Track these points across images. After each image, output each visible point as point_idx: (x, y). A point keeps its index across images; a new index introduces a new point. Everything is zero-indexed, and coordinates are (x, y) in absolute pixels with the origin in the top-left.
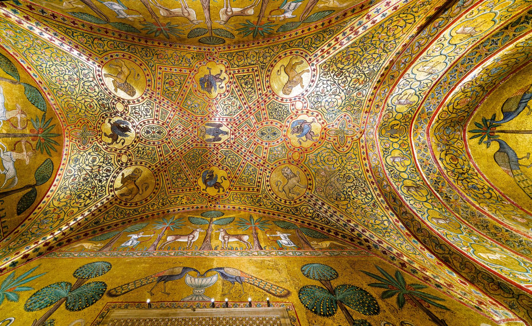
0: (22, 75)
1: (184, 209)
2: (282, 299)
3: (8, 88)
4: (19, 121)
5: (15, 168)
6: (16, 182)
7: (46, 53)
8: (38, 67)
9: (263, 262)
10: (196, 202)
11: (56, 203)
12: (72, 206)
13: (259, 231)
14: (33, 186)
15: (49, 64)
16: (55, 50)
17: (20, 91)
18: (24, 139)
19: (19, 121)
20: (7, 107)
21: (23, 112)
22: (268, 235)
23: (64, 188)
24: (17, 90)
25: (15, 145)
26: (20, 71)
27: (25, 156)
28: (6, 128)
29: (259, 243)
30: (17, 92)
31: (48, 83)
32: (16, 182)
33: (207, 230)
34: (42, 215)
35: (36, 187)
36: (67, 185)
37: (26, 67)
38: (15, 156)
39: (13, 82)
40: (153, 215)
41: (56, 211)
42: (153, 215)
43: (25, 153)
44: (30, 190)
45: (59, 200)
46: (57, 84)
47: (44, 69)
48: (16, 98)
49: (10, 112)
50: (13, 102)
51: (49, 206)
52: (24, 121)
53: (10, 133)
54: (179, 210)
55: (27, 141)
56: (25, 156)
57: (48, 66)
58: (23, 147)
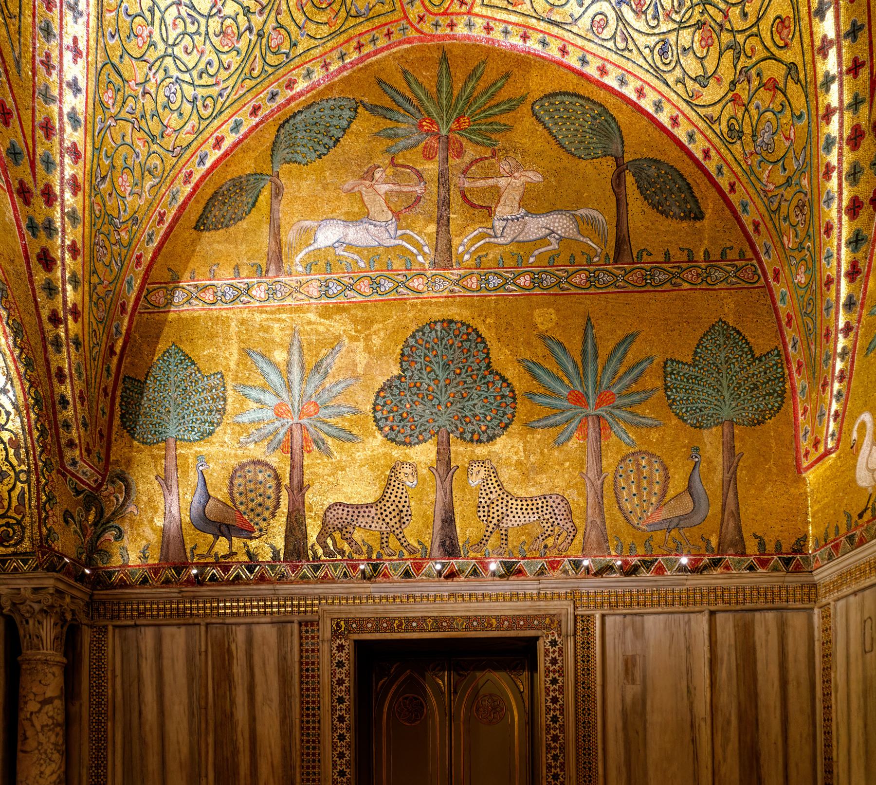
0: (247, 165)
3: (297, 207)
4: (396, 188)
5: (548, 213)
6: (595, 213)
7: (140, 79)
8: (205, 113)
11: (711, 93)
12: (752, 19)
14: (620, 168)
15: (174, 73)
16: (112, 42)
17: (300, 177)
18: (455, 180)
19: (396, 188)
20: (354, 214)
21: (369, 175)
23: (663, 53)
24: (299, 184)
25: (473, 206)
26: (234, 171)
27: (512, 183)
28: (420, 224)
30: (304, 185)
31: (249, 83)
32: (595, 213)
34: (737, 148)
35: (628, 158)
36: (652, 41)
37: (218, 153)
38: (508, 209)
39: (278, 192)
41: (745, 97)
43: (502, 182)
44: (629, 179)
45: (702, 80)
46: (242, 45)
47: (201, 92)
48: (325, 188)
49: (372, 210)
50: (338, 198)
51: (710, 120)
52: (395, 174)
53: (435, 215)
55: (464, 172)
56: (512, 183)
57: (187, 77)
58: (481, 183)
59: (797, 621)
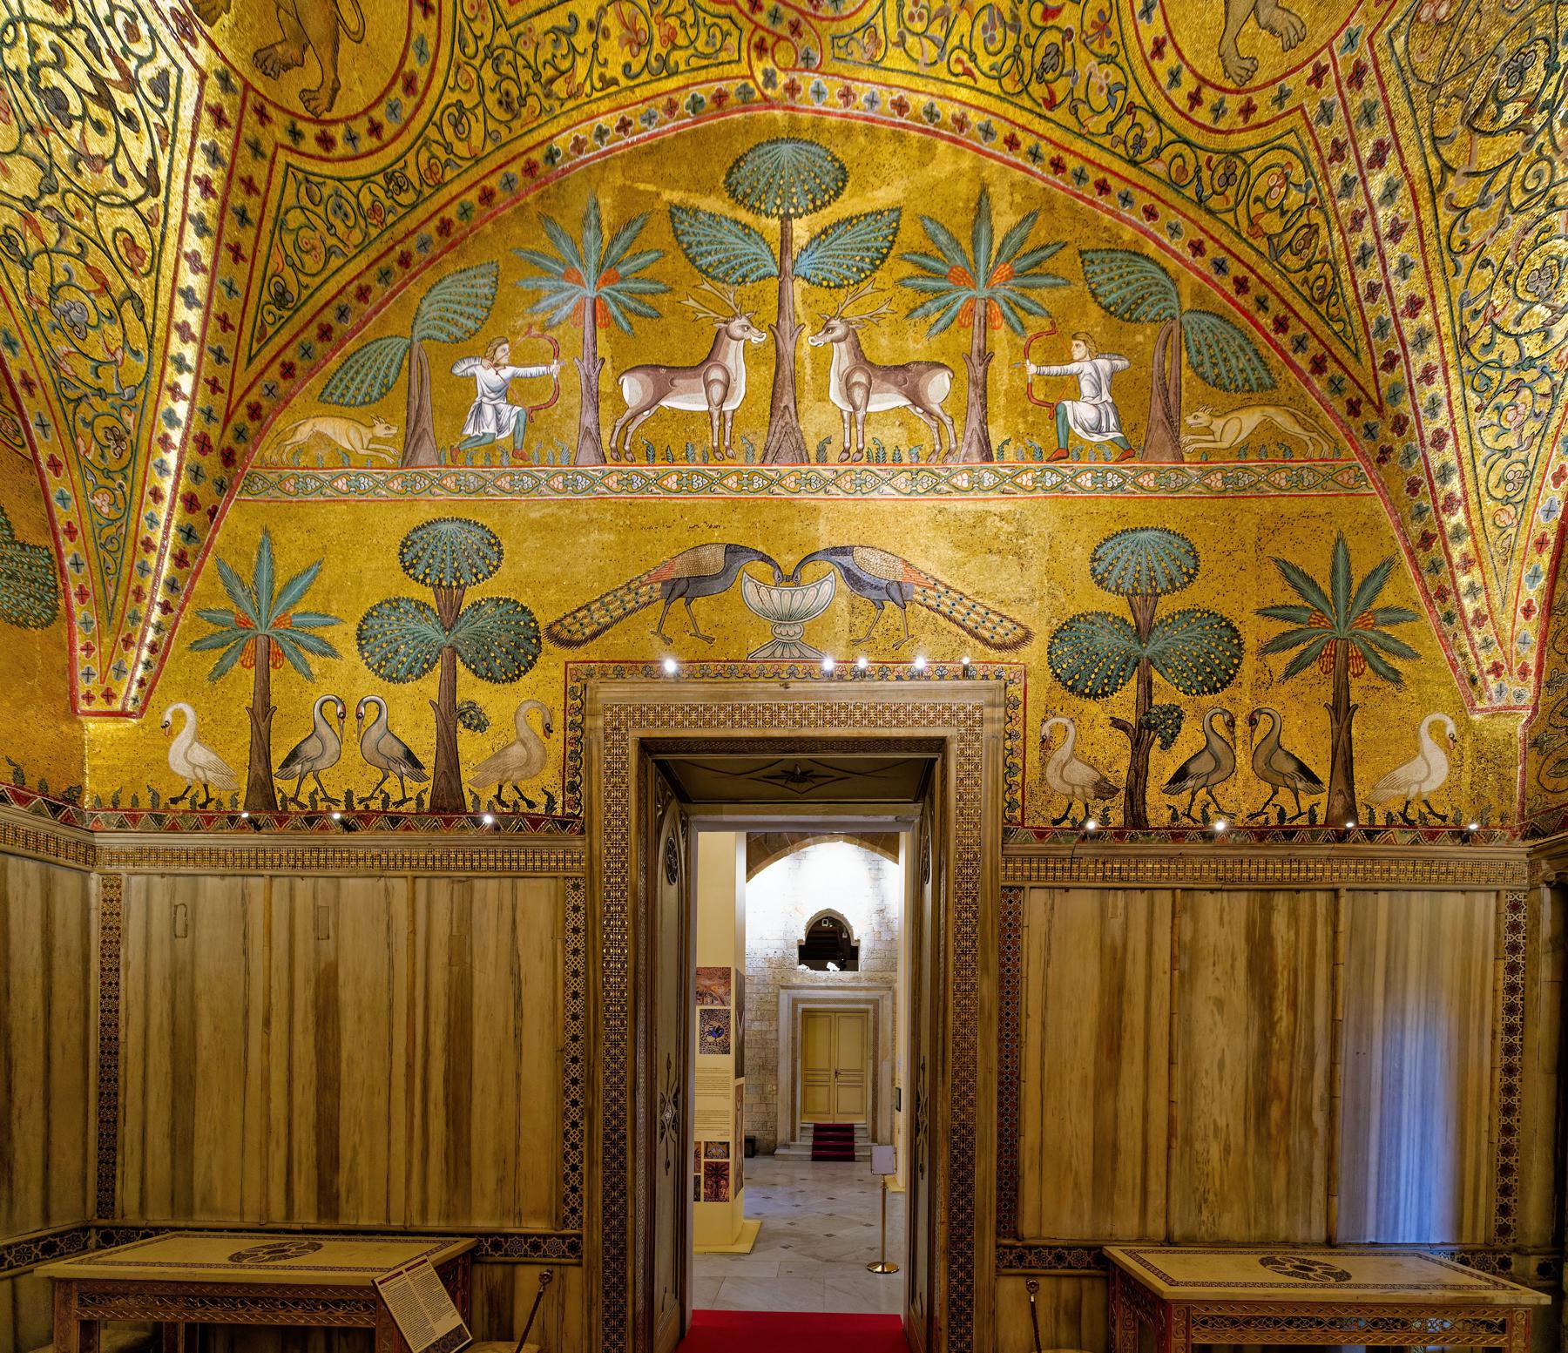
1: (624, 125)
2: (1004, 654)
9: (981, 518)
10: (678, 57)
13: (1000, 337)
22: (1032, 369)
29: (984, 422)
33: (775, 330)
40: (487, 196)
42: (487, 196)
54: (601, 133)
59: (67, 882)
